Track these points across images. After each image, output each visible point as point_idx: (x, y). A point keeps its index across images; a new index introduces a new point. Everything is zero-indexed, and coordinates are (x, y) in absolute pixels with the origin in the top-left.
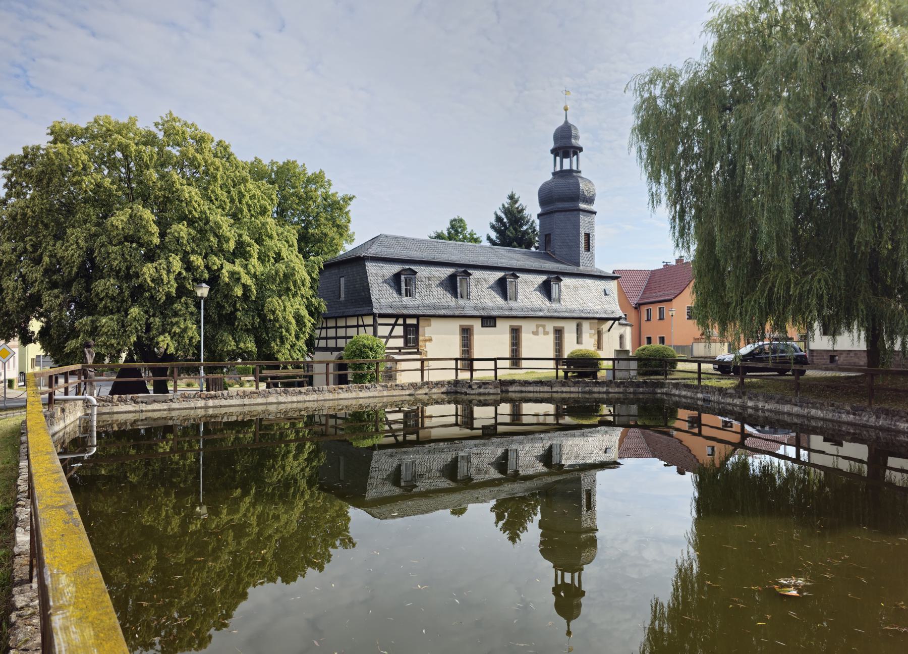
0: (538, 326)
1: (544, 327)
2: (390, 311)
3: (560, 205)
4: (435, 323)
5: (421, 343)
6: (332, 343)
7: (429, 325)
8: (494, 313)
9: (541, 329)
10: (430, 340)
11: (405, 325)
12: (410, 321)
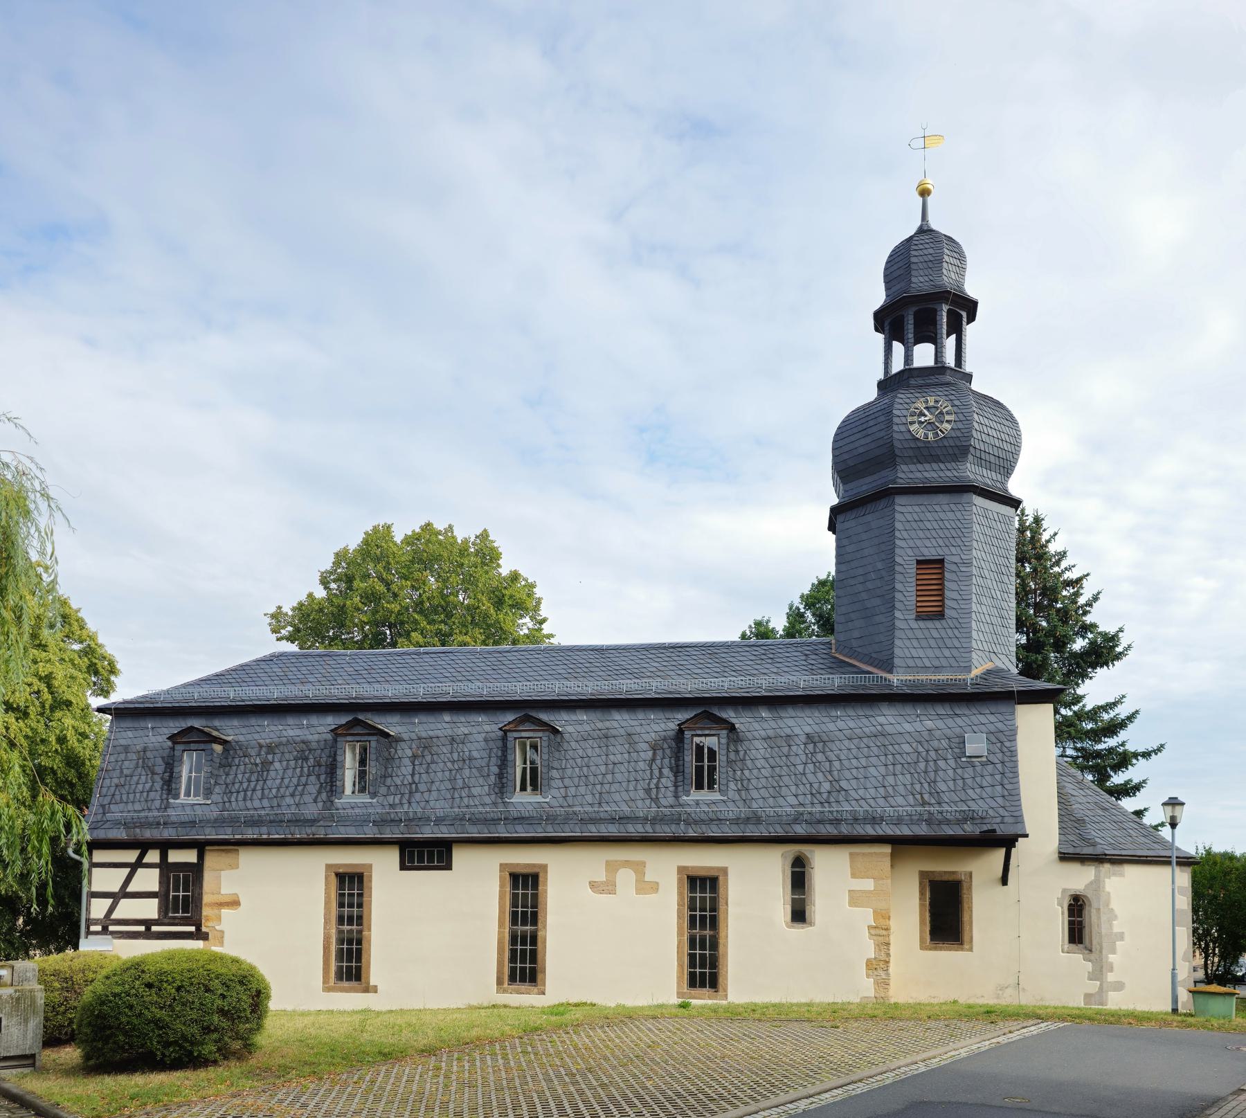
0: (612, 867)
1: (639, 868)
4: (249, 859)
5: (206, 912)
8: (444, 833)
9: (625, 878)
10: (234, 903)
11: (164, 866)
12: (175, 856)
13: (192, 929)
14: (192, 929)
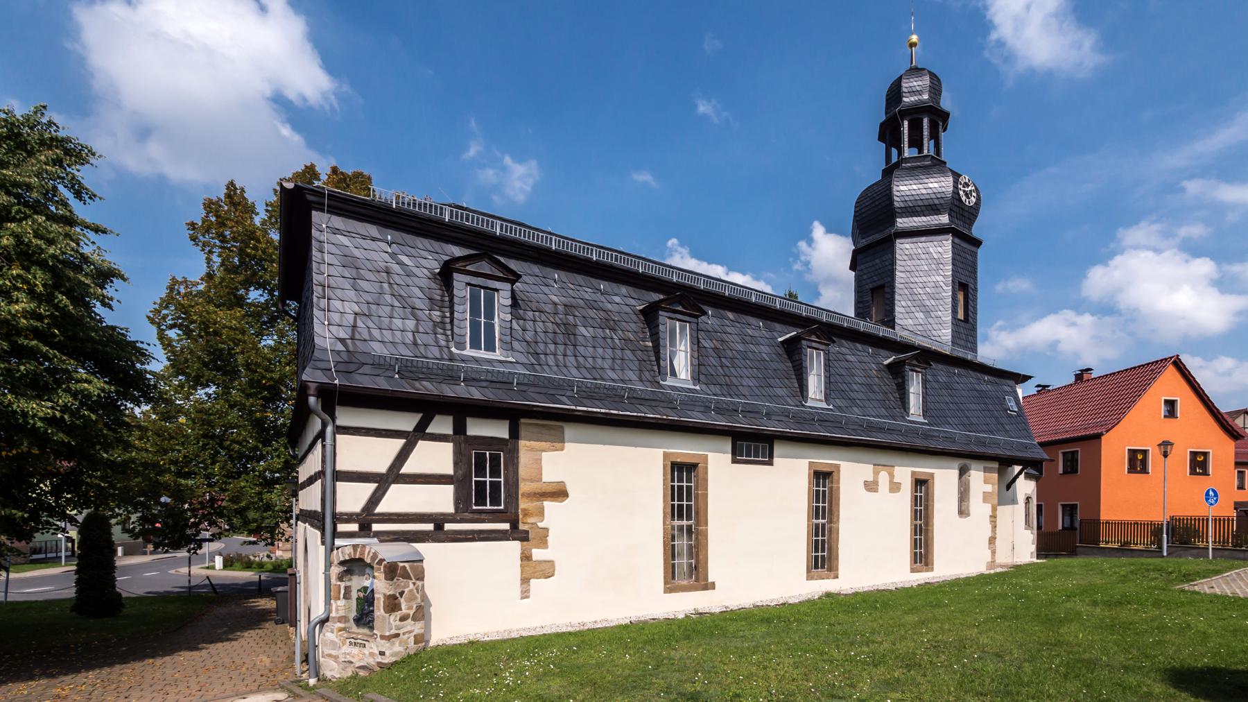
5: (523, 504)
10: (560, 493)
13: (506, 526)
14: (506, 526)
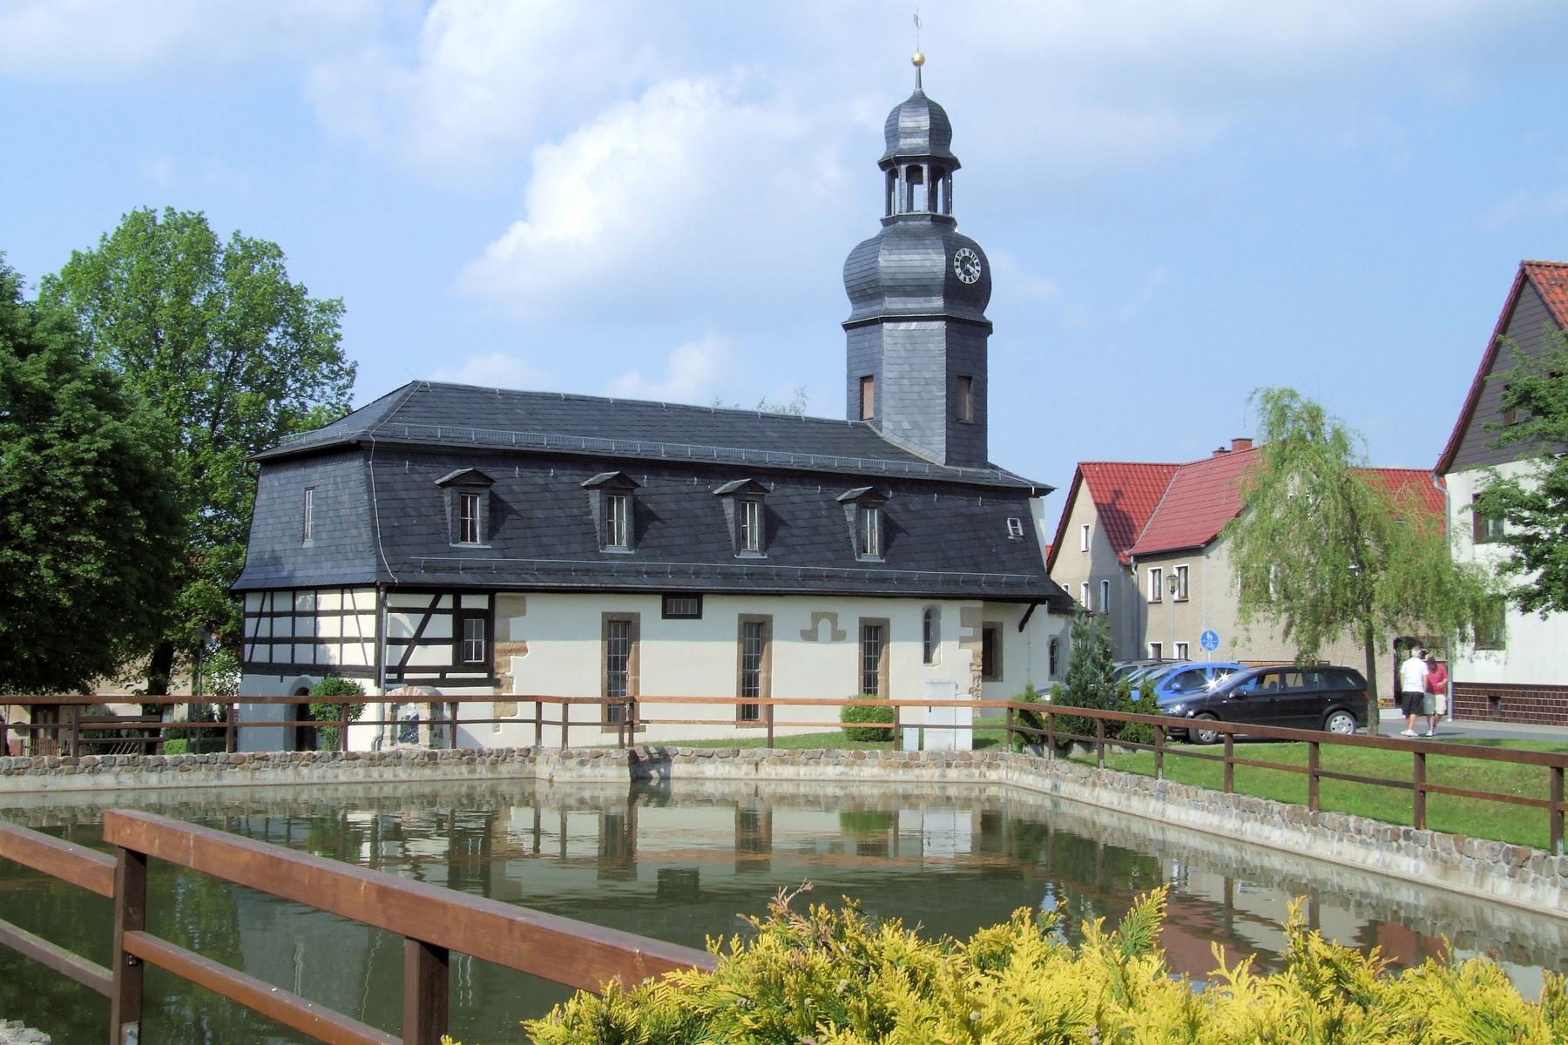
0: (816, 618)
1: (833, 618)
2: (424, 577)
3: (893, 304)
4: (534, 603)
5: (498, 659)
6: (282, 654)
7: (521, 612)
12: (468, 602)
13: (484, 675)
14: (484, 675)
